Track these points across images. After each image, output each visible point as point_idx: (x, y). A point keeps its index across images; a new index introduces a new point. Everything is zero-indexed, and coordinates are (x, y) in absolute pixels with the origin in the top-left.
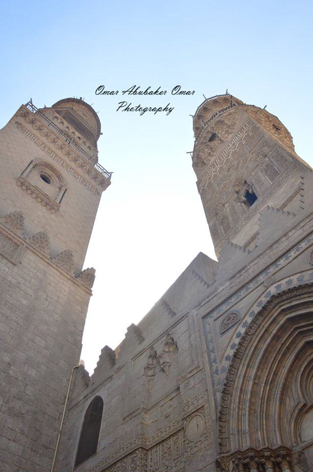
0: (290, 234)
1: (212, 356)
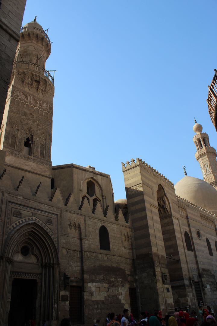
0: (46, 205)
1: (8, 221)
